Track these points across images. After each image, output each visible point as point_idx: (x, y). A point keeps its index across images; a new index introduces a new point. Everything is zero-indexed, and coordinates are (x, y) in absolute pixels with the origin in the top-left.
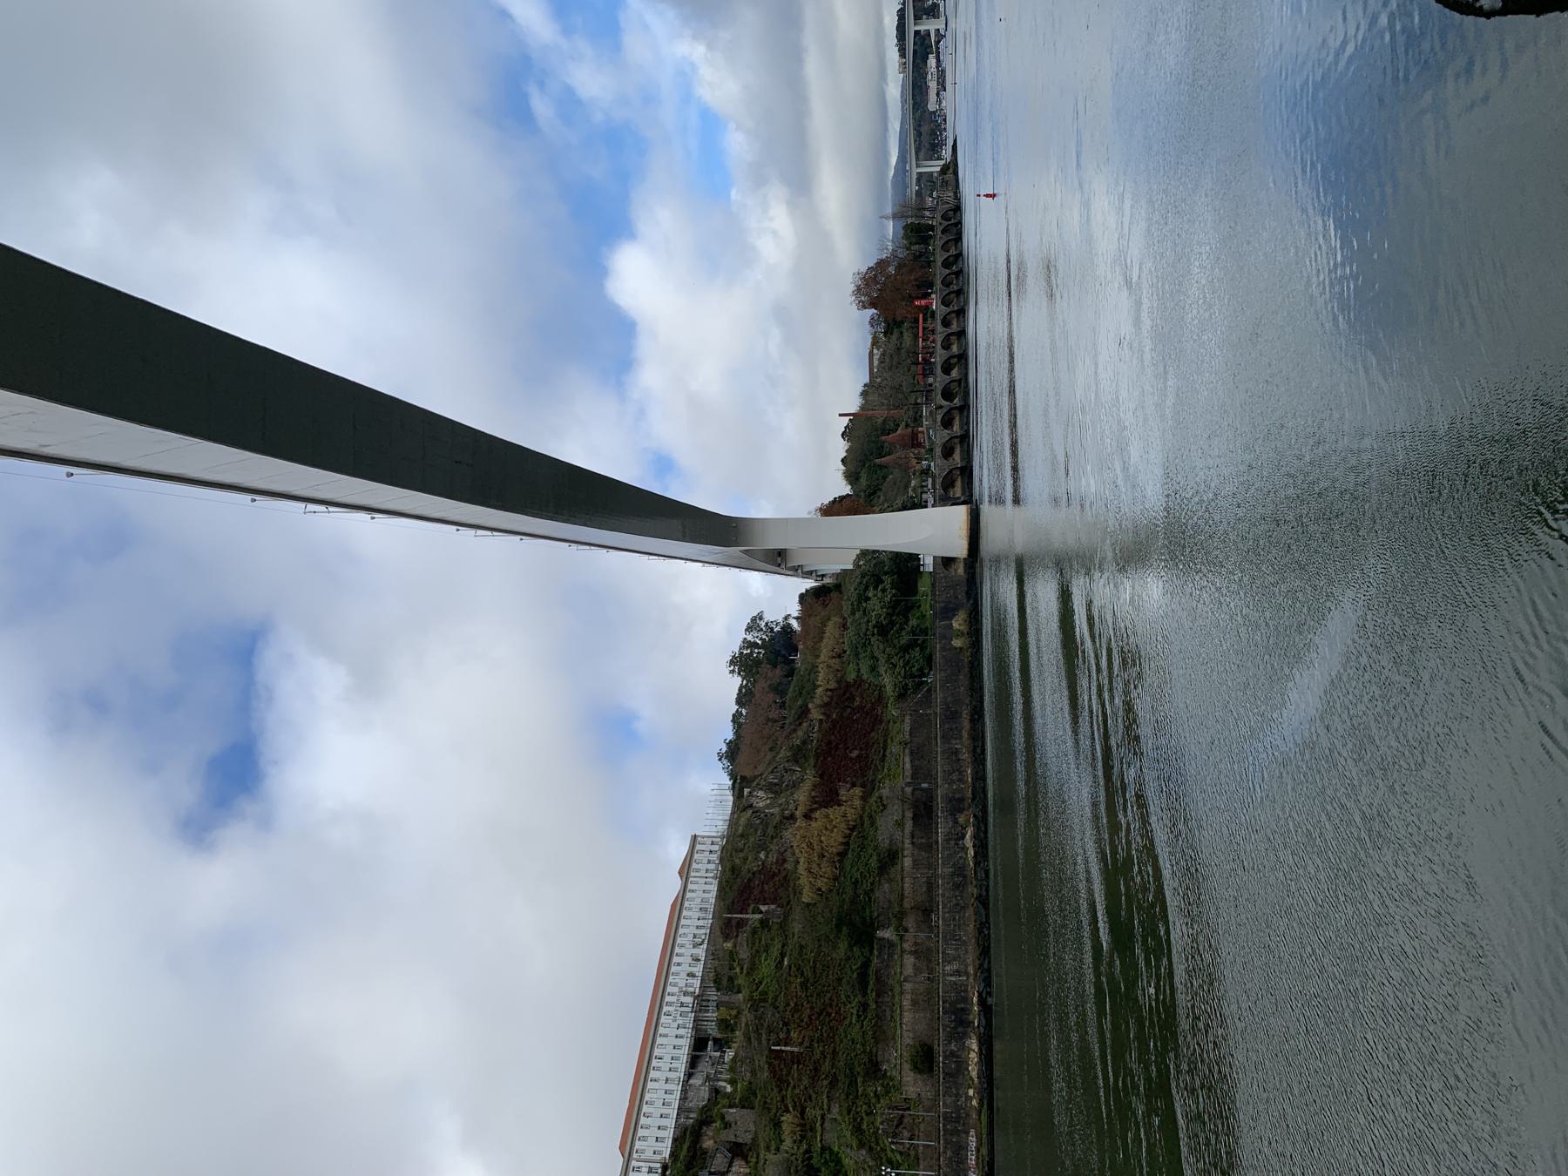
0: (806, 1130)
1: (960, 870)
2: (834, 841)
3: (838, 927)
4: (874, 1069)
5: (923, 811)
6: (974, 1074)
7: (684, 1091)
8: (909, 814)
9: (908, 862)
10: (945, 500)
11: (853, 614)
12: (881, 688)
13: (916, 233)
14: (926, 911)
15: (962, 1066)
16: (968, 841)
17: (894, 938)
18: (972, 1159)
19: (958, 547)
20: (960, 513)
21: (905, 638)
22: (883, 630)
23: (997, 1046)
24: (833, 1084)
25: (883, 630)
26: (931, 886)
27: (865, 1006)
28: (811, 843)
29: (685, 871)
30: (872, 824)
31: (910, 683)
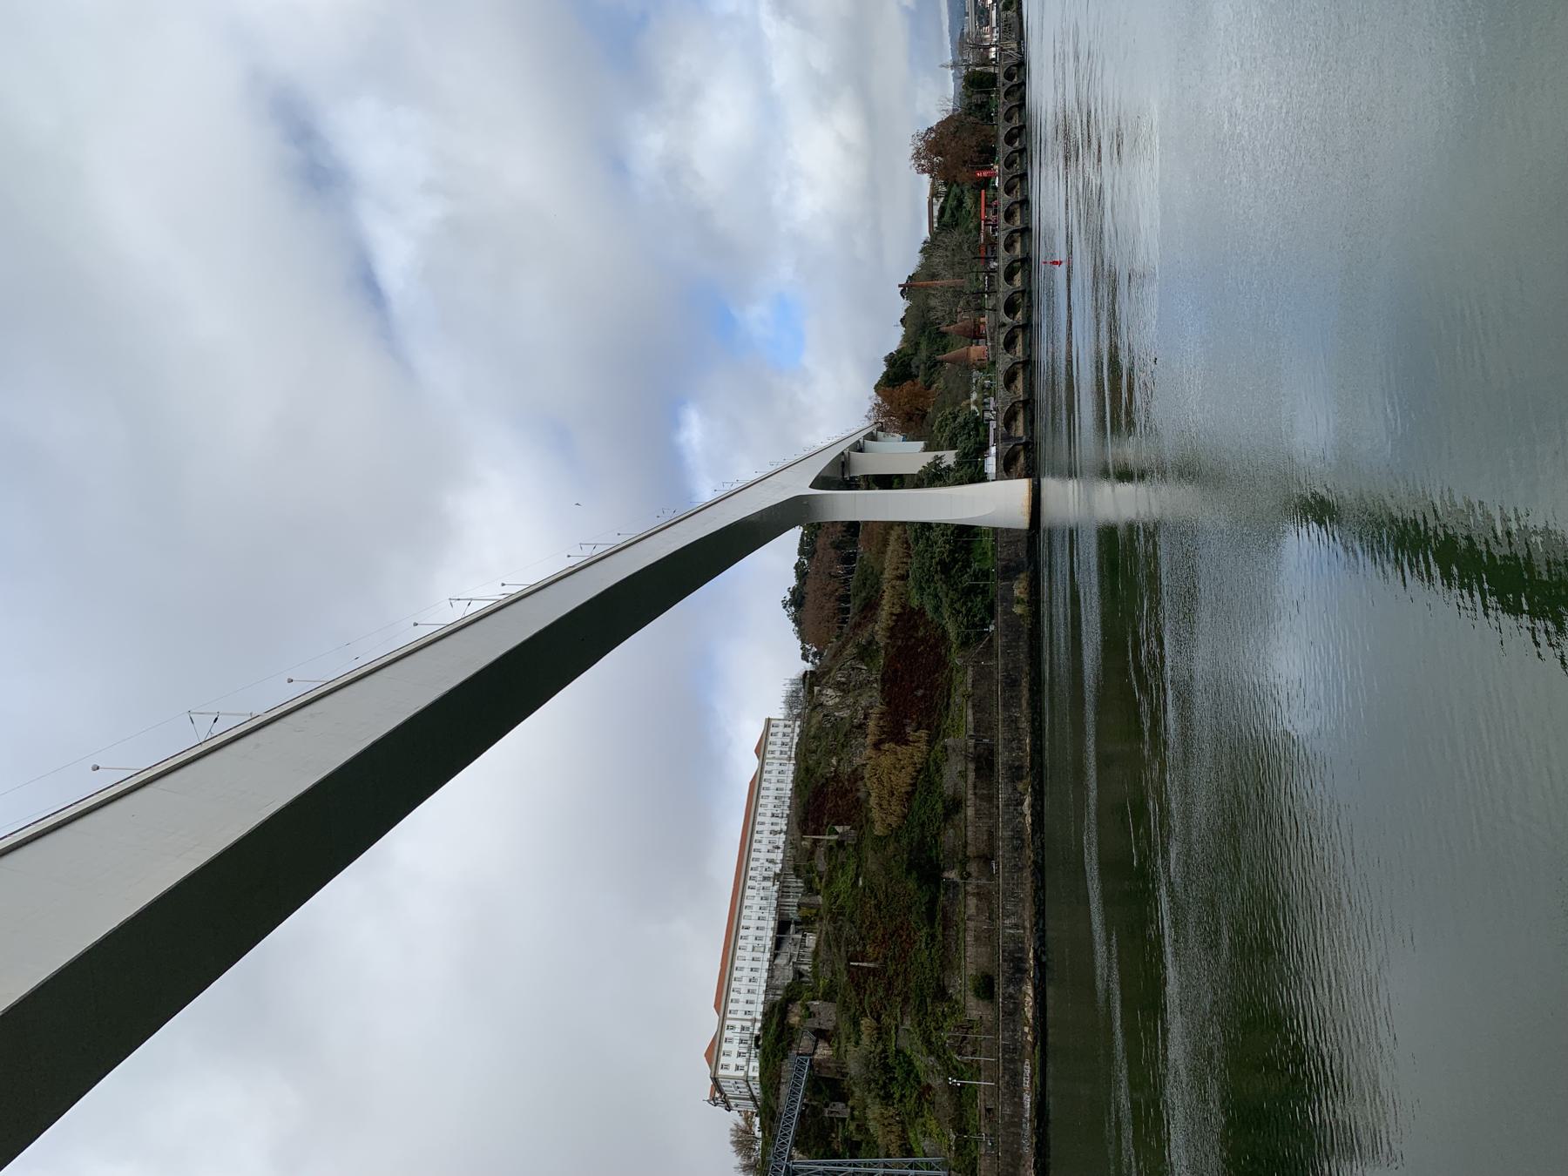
0: (881, 1033)
1: (1018, 834)
2: (903, 780)
3: (909, 872)
4: (942, 994)
5: (984, 763)
6: (1030, 1015)
7: (771, 970)
8: (972, 766)
9: (970, 812)
10: (1008, 469)
11: (917, 541)
12: (945, 631)
13: (977, 84)
14: (987, 859)
15: (1018, 1007)
16: (1026, 808)
17: (958, 880)
18: (1027, 1084)
19: (1021, 520)
20: (1022, 487)
21: (967, 581)
22: (945, 568)
23: (1050, 991)
24: (906, 1000)
25: (945, 568)
26: (991, 835)
27: (933, 937)
28: (883, 772)
29: (761, 750)
30: (938, 770)
31: (972, 632)
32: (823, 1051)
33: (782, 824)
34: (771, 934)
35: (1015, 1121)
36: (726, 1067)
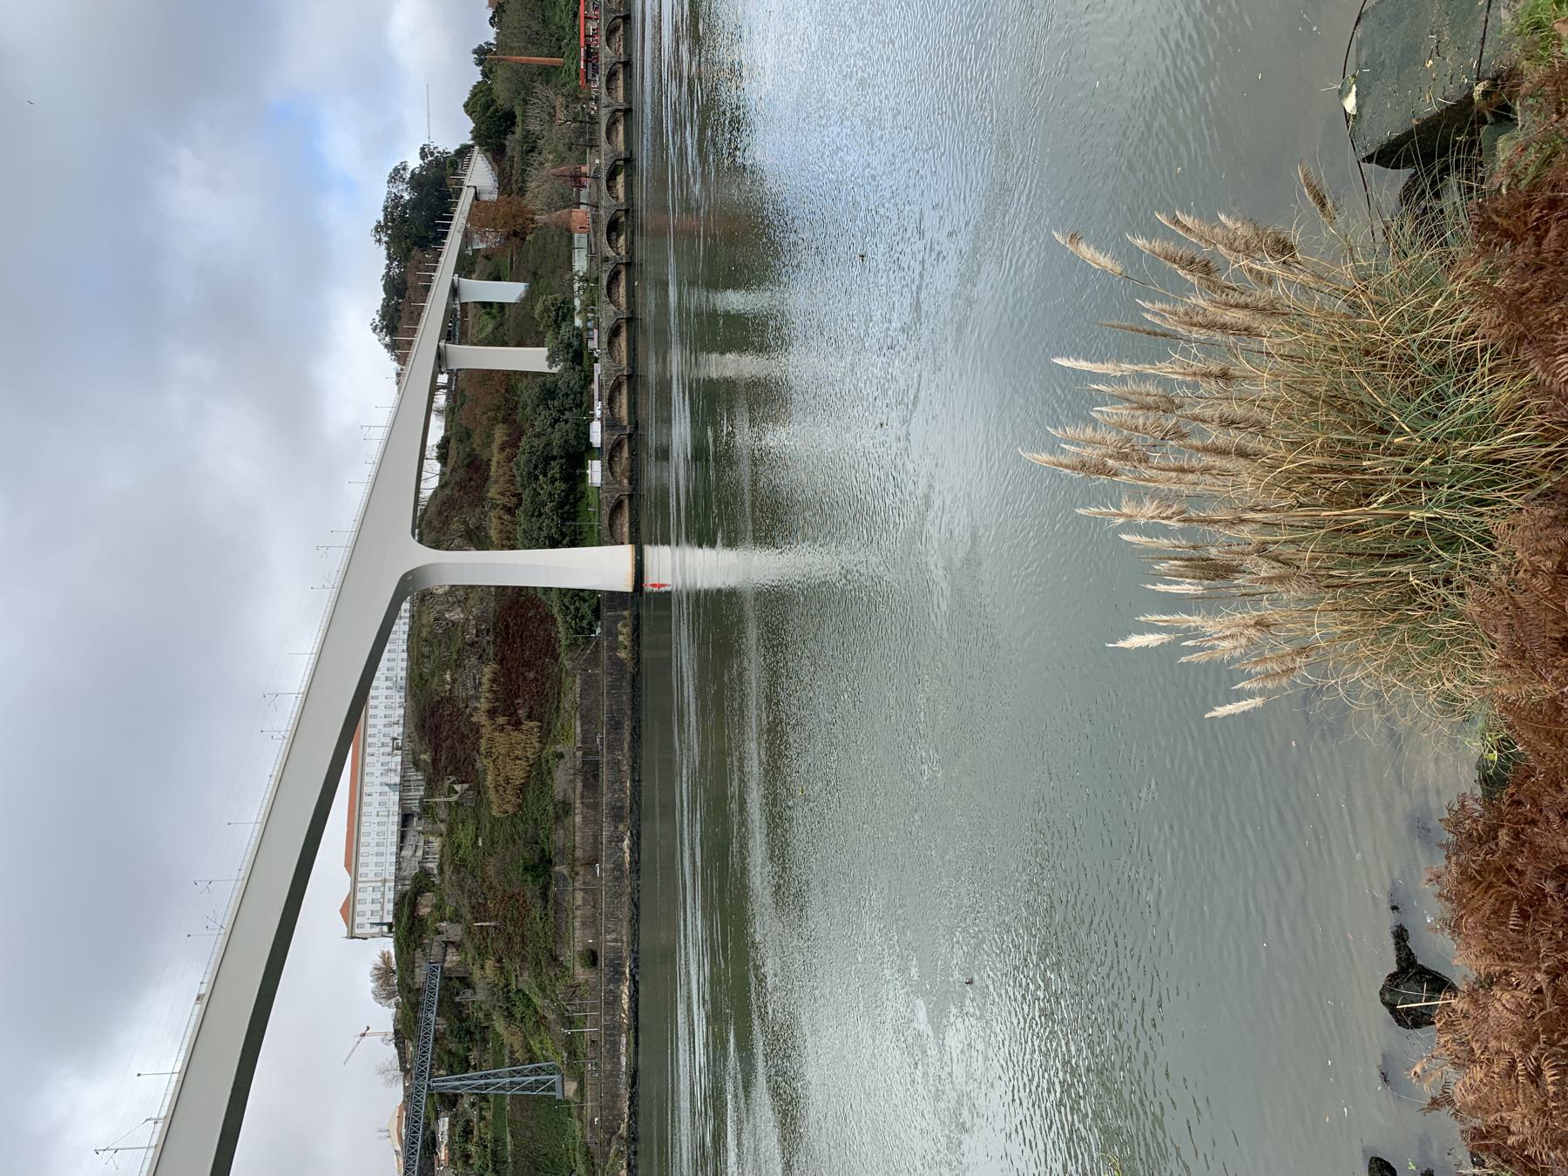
5: (590, 773)
7: (398, 863)
15: (617, 999)
18: (623, 1050)
19: (625, 584)
26: (596, 838)
32: (453, 958)
33: (398, 730)
34: (395, 828)
35: (614, 1074)
36: (361, 926)
